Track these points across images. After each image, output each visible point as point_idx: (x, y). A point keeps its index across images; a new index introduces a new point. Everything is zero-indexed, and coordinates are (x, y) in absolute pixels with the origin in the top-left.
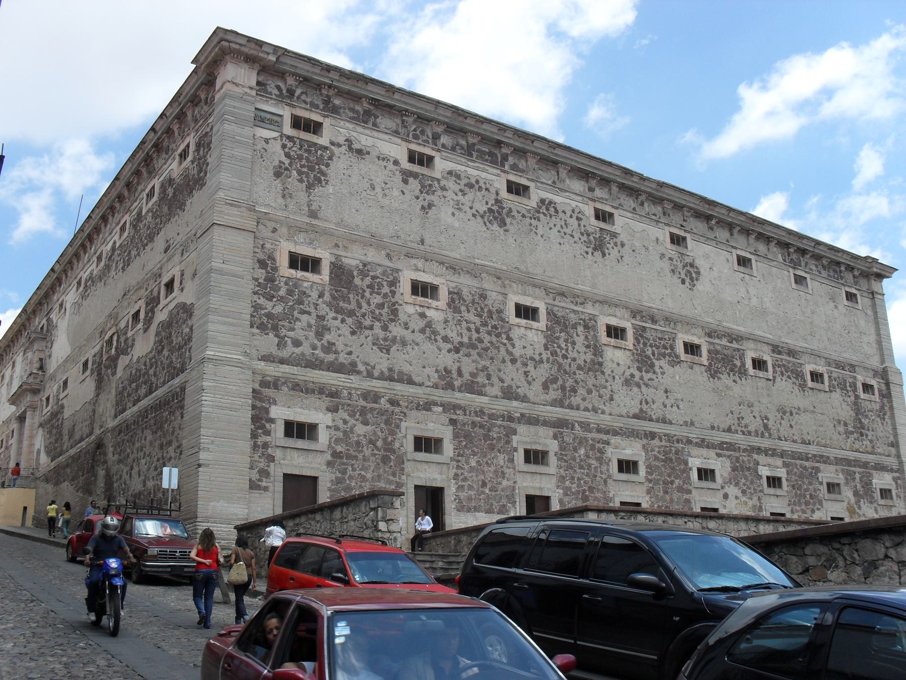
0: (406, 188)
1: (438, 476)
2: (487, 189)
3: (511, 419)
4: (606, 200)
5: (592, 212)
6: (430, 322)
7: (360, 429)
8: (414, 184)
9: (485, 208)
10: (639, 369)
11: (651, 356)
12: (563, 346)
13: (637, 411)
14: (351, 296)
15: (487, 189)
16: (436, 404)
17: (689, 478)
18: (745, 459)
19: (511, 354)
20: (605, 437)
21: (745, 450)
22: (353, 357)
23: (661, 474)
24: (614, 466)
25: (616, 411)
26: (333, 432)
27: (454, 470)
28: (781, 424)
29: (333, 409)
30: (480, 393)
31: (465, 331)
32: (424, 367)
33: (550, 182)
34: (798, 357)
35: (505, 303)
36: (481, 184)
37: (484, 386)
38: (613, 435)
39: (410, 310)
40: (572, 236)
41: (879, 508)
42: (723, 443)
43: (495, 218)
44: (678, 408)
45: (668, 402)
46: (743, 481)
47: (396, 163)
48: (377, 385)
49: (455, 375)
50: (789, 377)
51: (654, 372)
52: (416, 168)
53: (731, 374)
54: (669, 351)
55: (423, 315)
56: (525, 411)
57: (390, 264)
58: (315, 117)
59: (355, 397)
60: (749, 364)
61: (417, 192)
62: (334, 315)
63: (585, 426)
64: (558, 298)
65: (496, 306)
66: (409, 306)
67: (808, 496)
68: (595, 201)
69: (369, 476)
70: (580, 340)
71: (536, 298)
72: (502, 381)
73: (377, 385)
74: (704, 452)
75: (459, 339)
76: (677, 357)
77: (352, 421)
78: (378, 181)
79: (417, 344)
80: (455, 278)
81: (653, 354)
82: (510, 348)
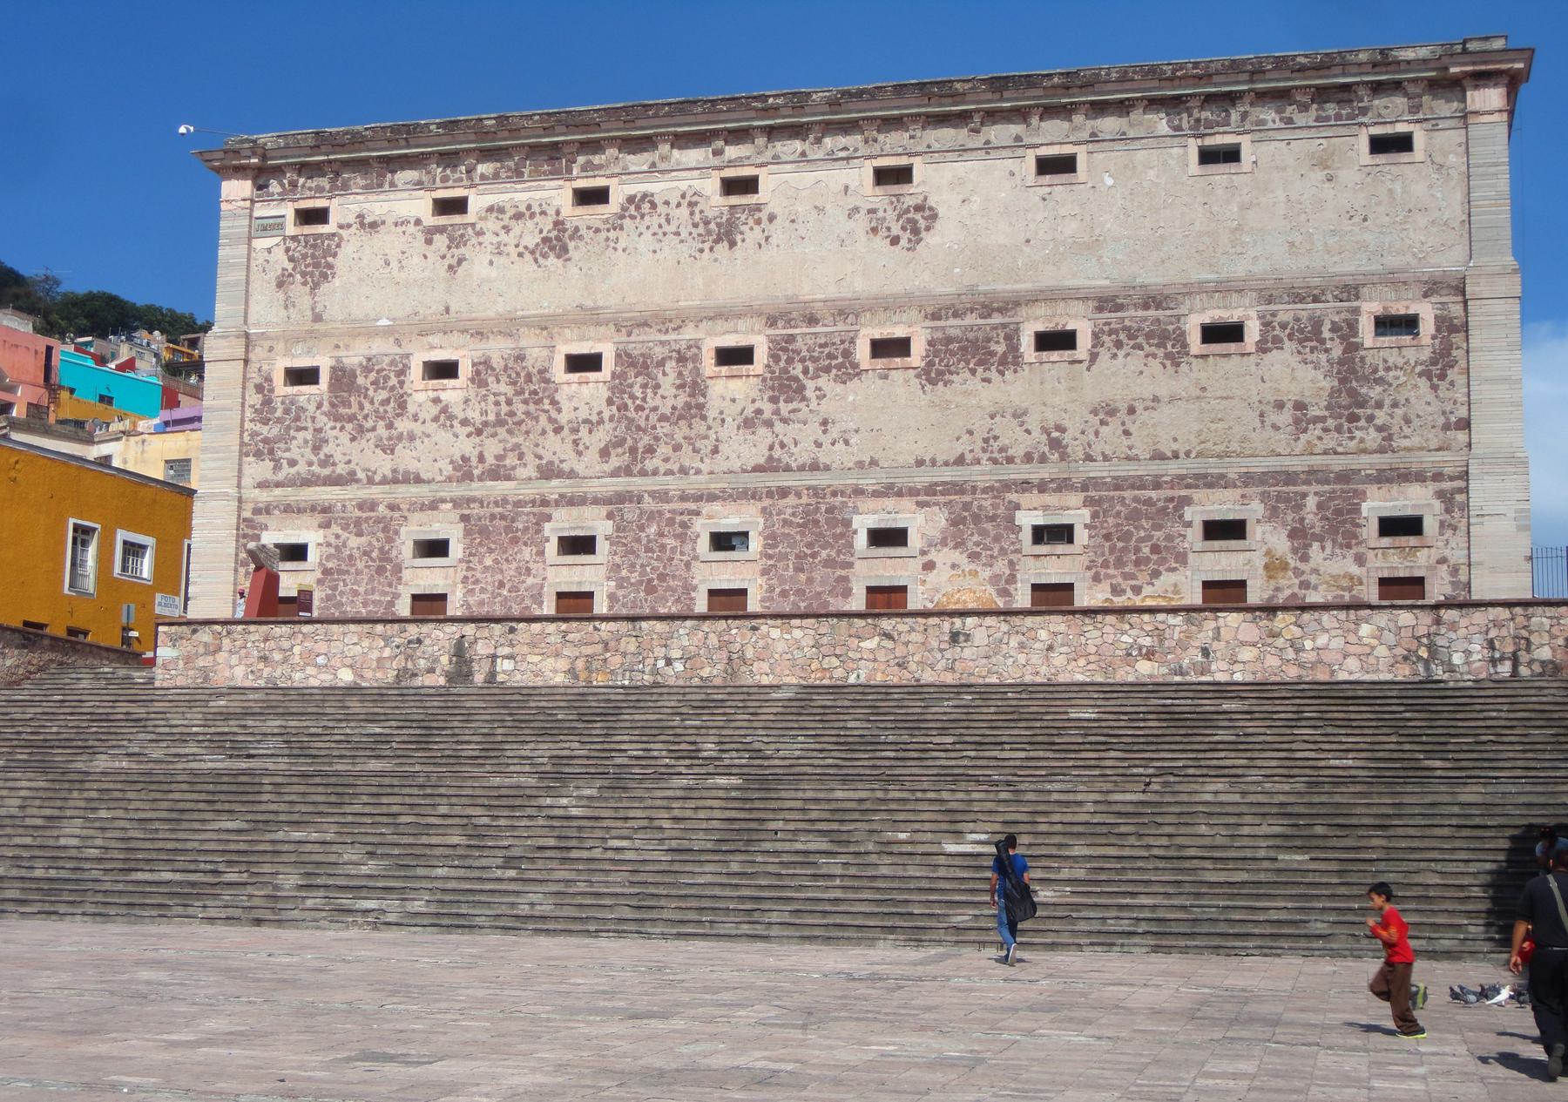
0: (429, 250)
1: (441, 582)
2: (543, 213)
3: (545, 503)
4: (749, 158)
5: (717, 184)
6: (447, 406)
7: (354, 542)
8: (441, 241)
9: (538, 240)
10: (774, 400)
11: (801, 376)
12: (639, 394)
13: (762, 461)
14: (352, 399)
15: (543, 213)
16: (443, 501)
18: (987, 504)
20: (692, 506)
21: (985, 490)
22: (352, 466)
23: (793, 545)
24: (704, 543)
25: (725, 466)
26: (324, 549)
27: (464, 573)
28: (1097, 433)
29: (326, 525)
30: (508, 478)
31: (491, 408)
32: (435, 460)
33: (645, 168)
34: (1172, 305)
35: (551, 359)
36: (536, 209)
37: (514, 468)
38: (707, 501)
40: (677, 234)
41: (1371, 554)
42: (936, 484)
43: (552, 248)
44: (847, 442)
45: (826, 440)
46: (976, 538)
47: (418, 222)
48: (375, 492)
49: (474, 461)
50: (1141, 348)
51: (804, 399)
53: (980, 370)
54: (840, 360)
55: (436, 401)
56: (564, 490)
58: (319, 203)
59: (350, 508)
60: (1027, 342)
61: (444, 250)
62: (331, 424)
63: (662, 496)
64: (636, 331)
65: (538, 366)
66: (420, 390)
67: (1146, 551)
68: (720, 168)
69: (362, 590)
70: (668, 382)
71: (599, 340)
72: (540, 458)
73: (375, 492)
74: (890, 503)
75: (484, 418)
76: (855, 366)
77: (345, 535)
79: (428, 436)
80: (482, 345)
81: (805, 371)
82: (554, 414)
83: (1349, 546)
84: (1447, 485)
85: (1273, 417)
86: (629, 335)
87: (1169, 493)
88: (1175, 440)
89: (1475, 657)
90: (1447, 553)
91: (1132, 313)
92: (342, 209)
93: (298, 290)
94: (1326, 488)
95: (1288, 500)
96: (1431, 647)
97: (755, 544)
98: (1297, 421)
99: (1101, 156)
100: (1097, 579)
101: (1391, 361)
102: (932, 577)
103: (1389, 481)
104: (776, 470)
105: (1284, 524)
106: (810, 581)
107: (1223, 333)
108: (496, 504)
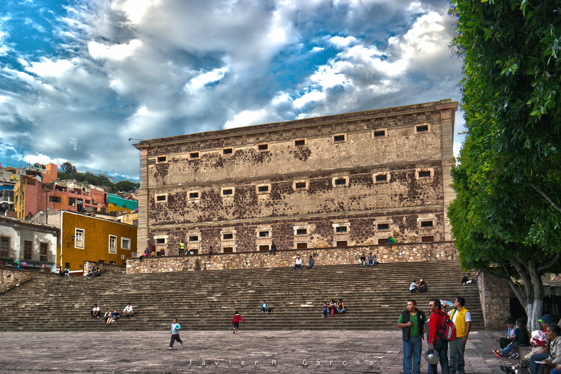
3: (220, 226)
5: (258, 147)
8: (193, 164)
10: (273, 199)
13: (271, 214)
15: (217, 156)
17: (293, 234)
19: (222, 206)
20: (255, 226)
21: (325, 219)
24: (258, 235)
25: (262, 216)
28: (351, 204)
35: (220, 191)
37: (212, 218)
39: (190, 202)
40: (249, 160)
41: (420, 231)
42: (313, 218)
43: (219, 165)
44: (291, 209)
45: (286, 208)
47: (187, 159)
52: (193, 159)
53: (322, 190)
55: (193, 203)
57: (184, 191)
58: (164, 156)
61: (193, 166)
63: (248, 224)
66: (189, 201)
70: (248, 196)
71: (231, 186)
72: (219, 215)
74: (302, 223)
76: (293, 190)
78: (182, 167)
81: (281, 192)
82: (221, 205)
83: (414, 229)
84: (438, 213)
85: (394, 198)
86: (238, 185)
87: (369, 218)
88: (370, 205)
89: (442, 255)
90: (439, 230)
91: (359, 174)
92: (169, 157)
93: (160, 178)
94: (408, 215)
95: (398, 218)
96: (431, 253)
97: (270, 234)
98: (400, 199)
99: (350, 135)
100: (352, 240)
101: (423, 183)
102: (313, 241)
103: (424, 213)
104: (274, 216)
105: (398, 224)
106: (284, 243)
107: (381, 178)
108: (209, 227)
